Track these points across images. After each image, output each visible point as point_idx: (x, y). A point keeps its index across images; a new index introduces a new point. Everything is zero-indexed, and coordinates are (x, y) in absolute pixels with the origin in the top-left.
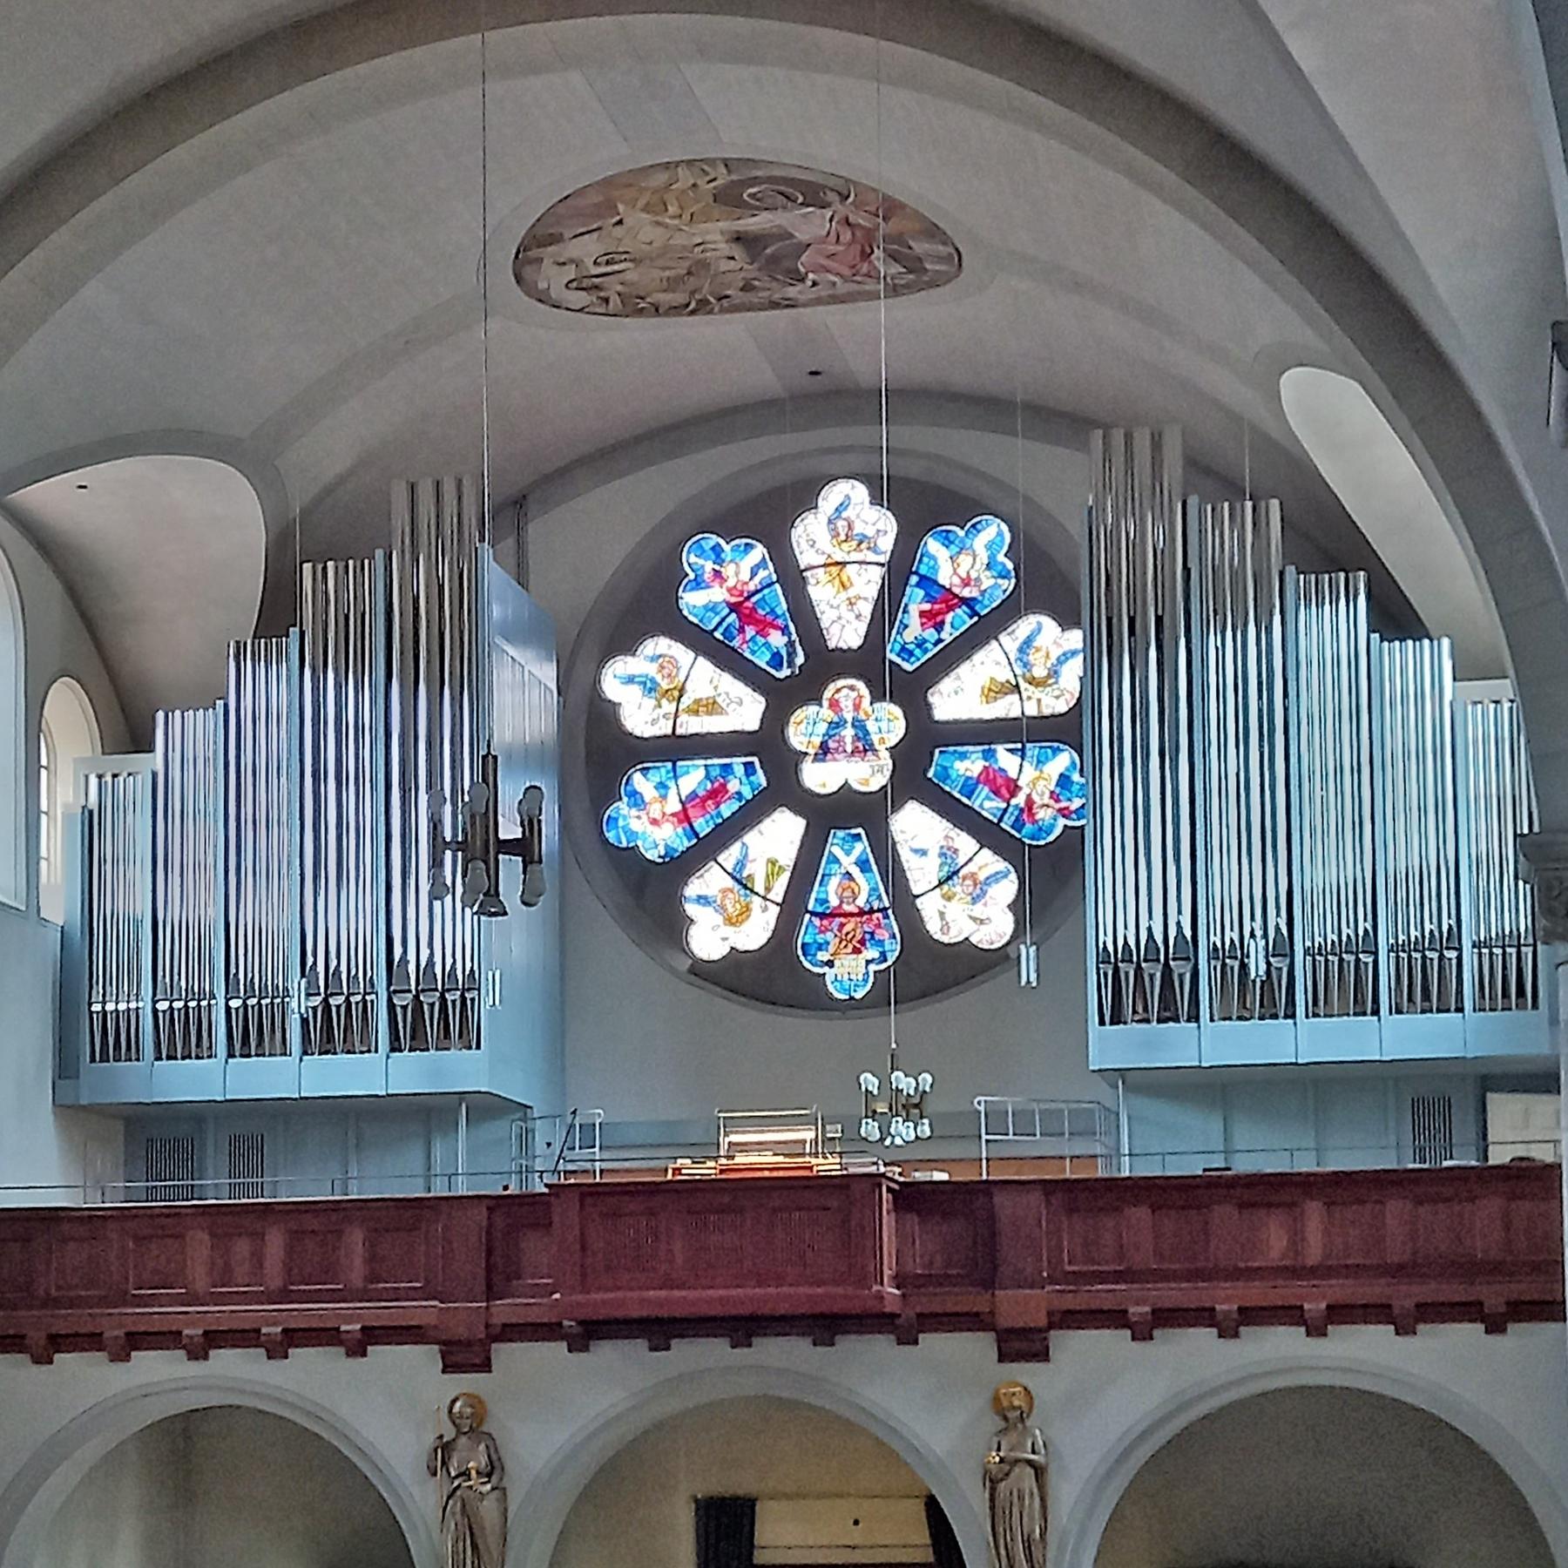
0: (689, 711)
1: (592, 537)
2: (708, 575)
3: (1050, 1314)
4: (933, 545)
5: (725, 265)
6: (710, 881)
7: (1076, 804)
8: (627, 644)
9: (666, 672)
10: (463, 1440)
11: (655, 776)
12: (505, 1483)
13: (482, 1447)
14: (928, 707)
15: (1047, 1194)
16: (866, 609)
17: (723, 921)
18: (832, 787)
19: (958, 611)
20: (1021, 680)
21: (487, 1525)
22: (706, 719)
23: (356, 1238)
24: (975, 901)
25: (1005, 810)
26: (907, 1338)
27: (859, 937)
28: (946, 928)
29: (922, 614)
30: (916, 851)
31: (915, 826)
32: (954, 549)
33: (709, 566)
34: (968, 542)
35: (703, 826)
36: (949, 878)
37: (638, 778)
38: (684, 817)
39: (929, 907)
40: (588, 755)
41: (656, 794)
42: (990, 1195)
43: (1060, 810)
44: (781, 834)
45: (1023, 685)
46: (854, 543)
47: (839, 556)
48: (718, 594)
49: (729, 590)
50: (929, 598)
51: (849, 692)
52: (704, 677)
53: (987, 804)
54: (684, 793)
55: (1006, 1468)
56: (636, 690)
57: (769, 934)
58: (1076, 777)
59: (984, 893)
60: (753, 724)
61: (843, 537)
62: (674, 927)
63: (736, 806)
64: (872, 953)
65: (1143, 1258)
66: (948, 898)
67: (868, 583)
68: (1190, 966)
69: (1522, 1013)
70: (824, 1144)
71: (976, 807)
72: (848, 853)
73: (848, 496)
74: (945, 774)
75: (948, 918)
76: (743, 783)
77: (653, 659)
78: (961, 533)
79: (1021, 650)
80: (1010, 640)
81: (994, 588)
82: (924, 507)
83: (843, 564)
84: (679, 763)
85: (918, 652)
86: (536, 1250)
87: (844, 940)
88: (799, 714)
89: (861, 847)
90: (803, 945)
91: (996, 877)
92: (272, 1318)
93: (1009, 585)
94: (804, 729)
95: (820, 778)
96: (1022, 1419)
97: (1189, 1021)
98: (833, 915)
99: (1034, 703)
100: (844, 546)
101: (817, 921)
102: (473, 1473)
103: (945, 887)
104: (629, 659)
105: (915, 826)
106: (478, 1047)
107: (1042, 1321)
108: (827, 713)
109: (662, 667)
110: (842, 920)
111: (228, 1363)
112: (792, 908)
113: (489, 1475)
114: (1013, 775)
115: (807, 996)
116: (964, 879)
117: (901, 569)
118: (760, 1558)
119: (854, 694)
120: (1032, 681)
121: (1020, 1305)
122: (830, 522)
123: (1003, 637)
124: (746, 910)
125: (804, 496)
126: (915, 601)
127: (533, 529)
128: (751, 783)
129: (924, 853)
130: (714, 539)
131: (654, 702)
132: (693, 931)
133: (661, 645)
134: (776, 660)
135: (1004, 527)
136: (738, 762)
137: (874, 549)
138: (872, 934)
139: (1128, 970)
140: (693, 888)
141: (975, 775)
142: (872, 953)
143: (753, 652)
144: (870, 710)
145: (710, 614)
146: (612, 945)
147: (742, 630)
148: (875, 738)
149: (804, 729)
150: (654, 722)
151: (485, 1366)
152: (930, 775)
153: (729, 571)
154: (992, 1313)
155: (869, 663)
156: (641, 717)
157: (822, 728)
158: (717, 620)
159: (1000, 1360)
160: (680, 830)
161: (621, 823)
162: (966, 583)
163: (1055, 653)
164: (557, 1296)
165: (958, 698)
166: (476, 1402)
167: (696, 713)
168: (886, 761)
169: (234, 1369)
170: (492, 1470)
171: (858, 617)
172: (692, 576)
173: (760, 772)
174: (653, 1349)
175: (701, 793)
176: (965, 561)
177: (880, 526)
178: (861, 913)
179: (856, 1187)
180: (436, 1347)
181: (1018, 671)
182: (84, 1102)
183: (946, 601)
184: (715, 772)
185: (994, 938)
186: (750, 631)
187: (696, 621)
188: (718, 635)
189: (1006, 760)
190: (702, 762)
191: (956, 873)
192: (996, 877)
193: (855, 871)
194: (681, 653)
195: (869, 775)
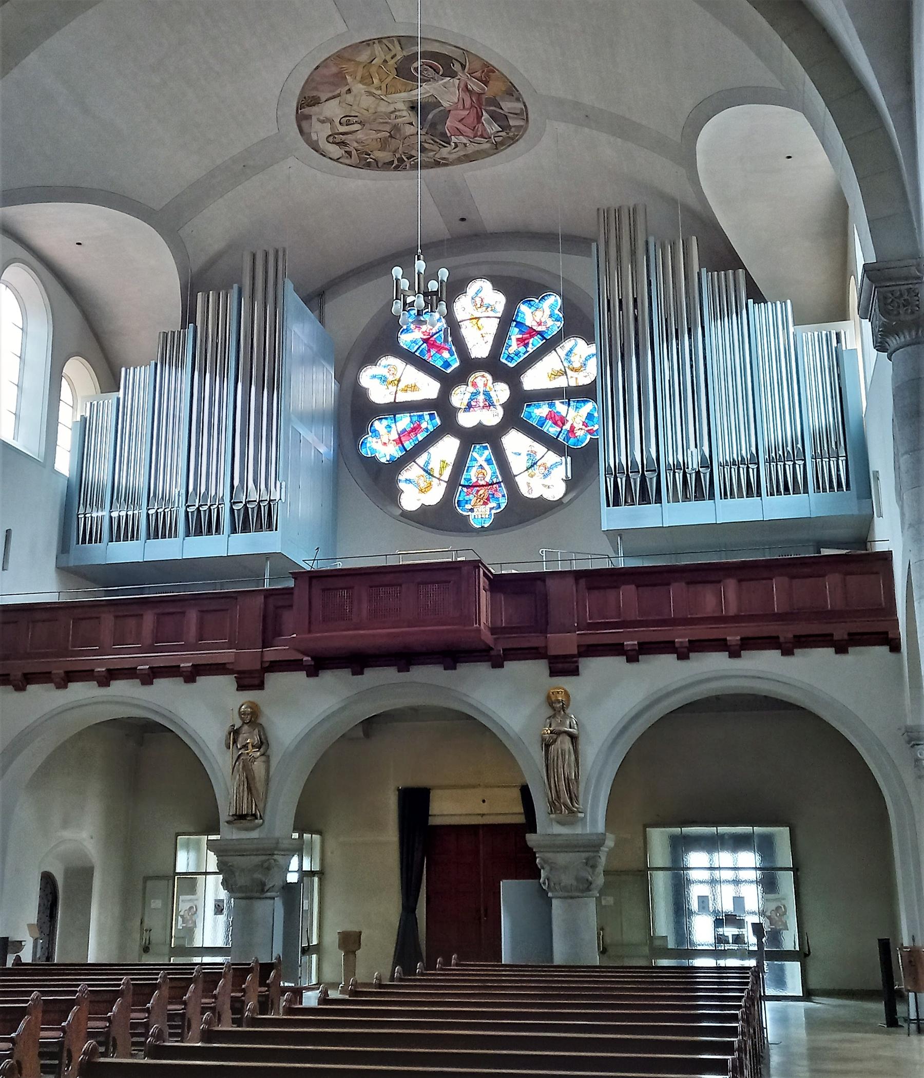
1: (354, 309)
4: (523, 308)
5: (409, 130)
6: (412, 472)
7: (596, 427)
10: (246, 727)
11: (385, 422)
12: (269, 752)
13: (256, 731)
14: (520, 383)
16: (490, 339)
17: (418, 491)
21: (257, 779)
23: (193, 616)
24: (545, 476)
26: (497, 664)
29: (518, 340)
35: (409, 445)
36: (532, 466)
37: (377, 425)
38: (399, 441)
40: (352, 412)
41: (386, 430)
42: (544, 581)
43: (588, 431)
44: (448, 447)
47: (477, 315)
50: (521, 332)
51: (482, 379)
52: (411, 374)
53: (551, 429)
54: (400, 430)
55: (555, 736)
56: (377, 381)
58: (596, 415)
59: (549, 473)
62: (392, 494)
63: (426, 434)
65: (633, 615)
67: (491, 327)
72: (481, 456)
76: (429, 423)
79: (567, 355)
80: (562, 350)
81: (554, 327)
82: (519, 290)
83: (479, 318)
85: (516, 358)
86: (289, 619)
87: (479, 498)
89: (488, 453)
91: (556, 465)
92: (145, 661)
93: (560, 324)
94: (459, 397)
95: (467, 420)
101: (465, 489)
102: (250, 746)
103: (530, 471)
112: (454, 483)
113: (260, 748)
117: (507, 320)
121: (563, 642)
124: (430, 486)
126: (515, 333)
127: (329, 307)
136: (426, 415)
139: (622, 482)
140: (404, 475)
142: (493, 504)
146: (358, 498)
147: (429, 351)
148: (494, 399)
149: (459, 397)
154: (546, 647)
155: (493, 365)
156: (379, 395)
157: (468, 396)
161: (368, 445)
162: (539, 324)
165: (533, 380)
168: (500, 412)
170: (263, 744)
174: (354, 674)
176: (539, 314)
178: (488, 485)
179: (465, 570)
181: (566, 364)
183: (530, 333)
184: (415, 419)
189: (560, 407)
191: (535, 463)
192: (556, 465)
193: (485, 465)
195: (492, 418)
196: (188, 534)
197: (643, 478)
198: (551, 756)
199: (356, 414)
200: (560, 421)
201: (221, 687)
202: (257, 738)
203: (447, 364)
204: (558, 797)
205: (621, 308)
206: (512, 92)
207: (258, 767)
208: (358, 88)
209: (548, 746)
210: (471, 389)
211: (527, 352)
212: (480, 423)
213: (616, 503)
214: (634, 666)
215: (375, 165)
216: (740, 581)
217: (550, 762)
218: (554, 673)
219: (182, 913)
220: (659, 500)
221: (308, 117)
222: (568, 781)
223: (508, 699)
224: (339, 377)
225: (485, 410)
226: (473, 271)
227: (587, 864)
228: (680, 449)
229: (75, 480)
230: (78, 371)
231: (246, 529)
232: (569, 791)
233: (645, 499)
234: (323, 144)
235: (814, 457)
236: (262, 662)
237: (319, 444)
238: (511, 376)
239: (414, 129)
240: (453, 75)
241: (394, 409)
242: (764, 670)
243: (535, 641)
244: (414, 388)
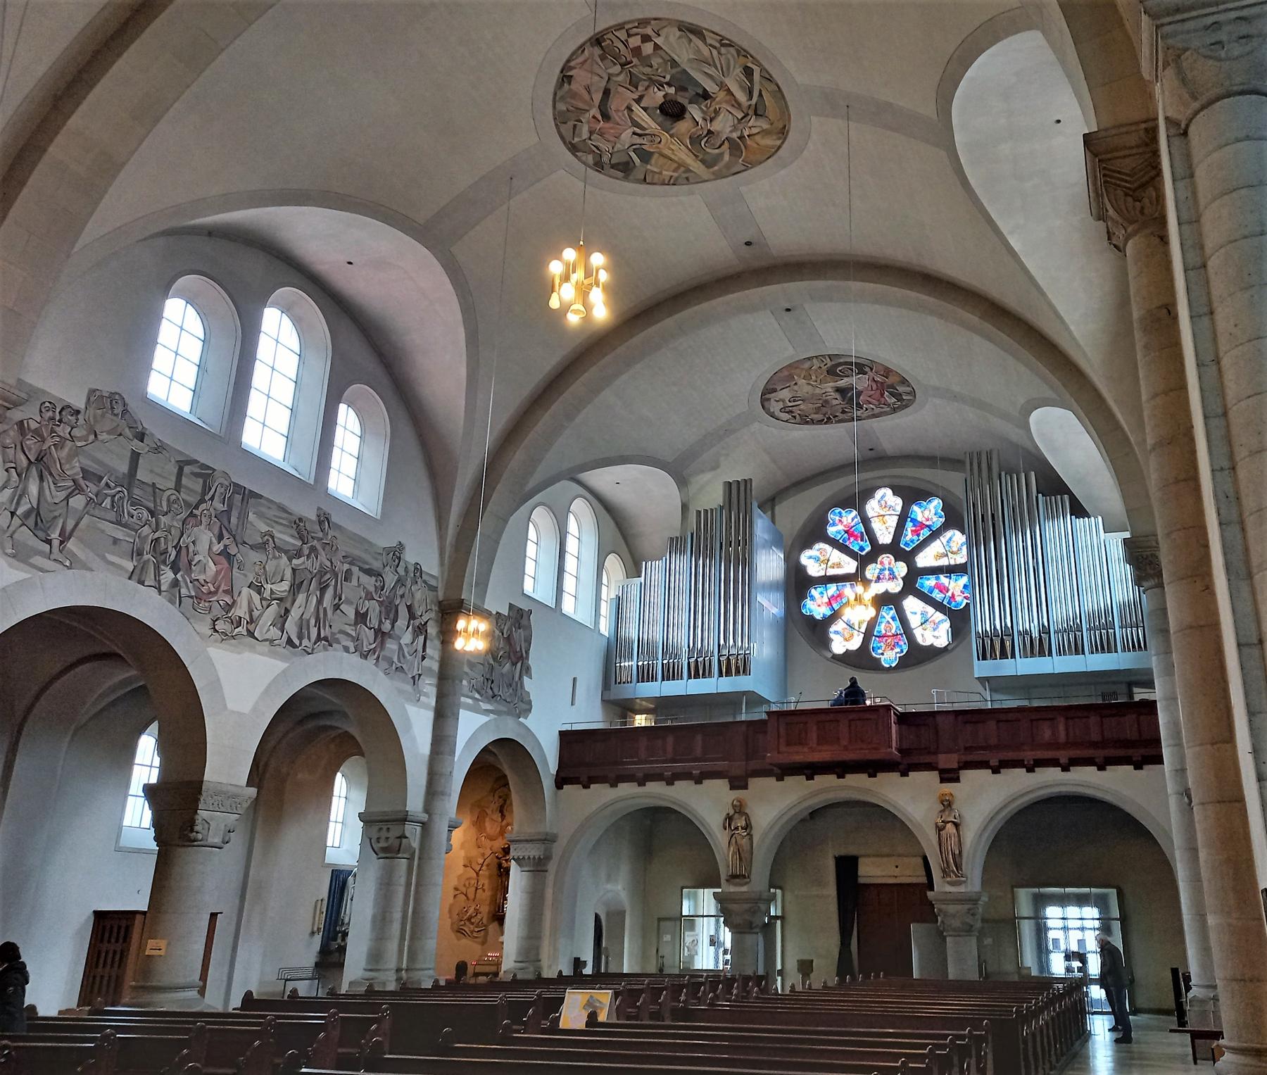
1: (795, 512)
6: (838, 626)
8: (807, 543)
16: (892, 530)
17: (842, 642)
26: (904, 774)
28: (924, 640)
37: (813, 592)
38: (829, 603)
48: (840, 527)
51: (887, 559)
52: (836, 556)
53: (937, 595)
60: (853, 570)
62: (825, 642)
64: (898, 650)
67: (893, 522)
73: (885, 494)
81: (938, 522)
82: (911, 495)
89: (893, 612)
91: (942, 621)
98: (884, 636)
105: (912, 605)
108: (879, 566)
112: (868, 635)
124: (852, 635)
125: (868, 493)
126: (909, 525)
127: (777, 508)
133: (822, 545)
134: (862, 549)
140: (833, 628)
142: (898, 650)
146: (803, 647)
151: (745, 787)
153: (844, 519)
155: (895, 549)
156: (814, 570)
159: (941, 782)
169: (656, 792)
170: (748, 827)
176: (926, 513)
182: (612, 698)
189: (943, 579)
192: (942, 621)
196: (690, 677)
197: (1002, 640)
199: (798, 583)
200: (943, 589)
201: (721, 785)
202: (744, 823)
203: (862, 549)
206: (904, 381)
208: (802, 382)
210: (879, 566)
213: (984, 658)
215: (813, 422)
220: (1013, 656)
221: (769, 399)
222: (953, 854)
224: (786, 559)
226: (878, 483)
228: (1027, 622)
229: (613, 639)
230: (613, 562)
233: (1004, 655)
234: (777, 413)
237: (771, 606)
238: (906, 556)
239: (836, 400)
240: (865, 373)
244: (839, 565)
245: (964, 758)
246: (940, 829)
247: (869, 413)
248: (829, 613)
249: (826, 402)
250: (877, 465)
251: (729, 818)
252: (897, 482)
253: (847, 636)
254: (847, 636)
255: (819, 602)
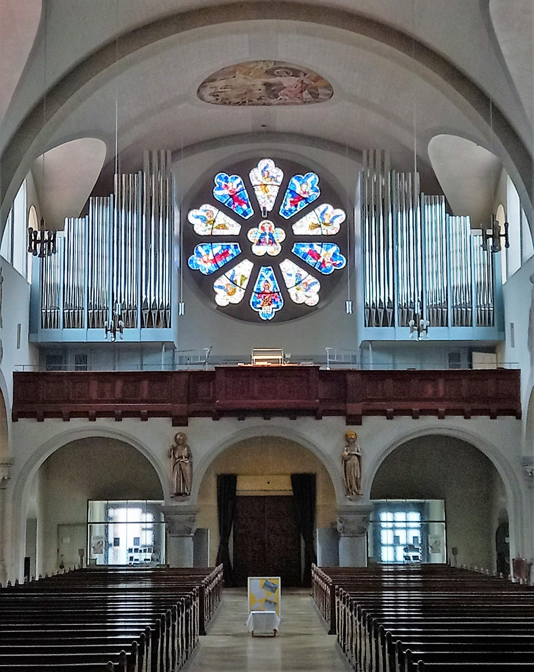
0: (216, 228)
1: (186, 173)
2: (223, 186)
3: (363, 410)
4: (294, 180)
6: (222, 281)
7: (338, 262)
9: (209, 215)
10: (179, 447)
13: (186, 449)
15: (362, 374)
16: (273, 199)
18: (262, 253)
19: (302, 201)
20: (321, 224)
22: (222, 230)
24: (307, 290)
25: (316, 263)
26: (319, 418)
27: (270, 300)
28: (297, 298)
29: (291, 202)
30: (288, 275)
31: (288, 267)
32: (301, 182)
33: (224, 183)
34: (305, 181)
35: (221, 264)
36: (299, 282)
37: (200, 248)
38: (214, 261)
39: (292, 292)
41: (205, 253)
42: (345, 375)
43: (333, 264)
44: (245, 268)
45: (322, 225)
46: (269, 179)
47: (265, 182)
48: (226, 192)
49: (230, 191)
50: (293, 197)
51: (267, 224)
52: (221, 218)
53: (310, 261)
56: (199, 220)
57: (242, 299)
58: (338, 254)
59: (309, 288)
60: (237, 232)
61: (266, 177)
63: (231, 258)
64: (275, 306)
66: (298, 289)
67: (274, 191)
68: (392, 310)
69: (489, 328)
70: (285, 359)
71: (307, 262)
74: (297, 251)
75: (298, 295)
77: (205, 211)
78: (303, 178)
79: (321, 214)
82: (292, 169)
83: (266, 185)
84: (213, 244)
85: (289, 213)
87: (266, 301)
88: (252, 230)
89: (272, 272)
90: (253, 302)
91: (313, 284)
93: (318, 194)
94: (253, 235)
95: (258, 250)
96: (354, 442)
97: (391, 326)
99: (325, 231)
100: (267, 179)
101: (257, 295)
102: (184, 457)
103: (298, 286)
104: (197, 210)
105: (288, 267)
106: (170, 327)
107: (360, 412)
108: (262, 232)
109: (207, 214)
110: (265, 295)
111: (101, 422)
114: (319, 252)
115: (255, 318)
116: (304, 283)
117: (284, 188)
118: (238, 494)
119: (269, 225)
120: (325, 224)
121: (354, 408)
122: (262, 172)
123: (316, 210)
124: (234, 291)
126: (289, 198)
128: (236, 251)
129: (291, 275)
130: (225, 175)
131: (205, 225)
132: (217, 296)
133: (207, 207)
135: (317, 177)
136: (232, 245)
137: (276, 181)
138: (274, 300)
140: (217, 283)
141: (307, 252)
143: (237, 211)
144: (274, 230)
145: (224, 198)
147: (234, 204)
148: (276, 239)
149: (253, 235)
150: (205, 231)
152: (293, 251)
153: (230, 185)
155: (274, 216)
156: (201, 229)
157: (259, 235)
158: (225, 200)
160: (213, 265)
161: (194, 262)
162: (305, 193)
163: (332, 216)
164: (218, 401)
165: (301, 228)
166: (182, 435)
167: (219, 229)
170: (189, 456)
171: (271, 201)
172: (218, 186)
173: (239, 248)
175: (220, 253)
176: (304, 186)
177: (278, 174)
178: (271, 293)
180: (171, 418)
181: (321, 221)
184: (225, 247)
185: (312, 302)
186: (236, 204)
187: (219, 200)
188: (226, 205)
189: (316, 247)
190: (221, 244)
191: (300, 282)
192: (313, 284)
193: (269, 280)
194: (215, 211)
195: (274, 250)
197: (385, 311)
198: (347, 466)
201: (164, 423)
203: (245, 213)
204: (351, 486)
205: (375, 210)
207: (188, 468)
209: (346, 461)
211: (296, 210)
212: (266, 253)
214: (389, 421)
216: (446, 380)
217: (347, 469)
218: (348, 423)
219: (93, 545)
220: (393, 325)
223: (323, 437)
225: (270, 245)
227: (363, 520)
231: (150, 325)
232: (357, 484)
233: (385, 324)
235: (477, 307)
236: (188, 411)
238: (286, 225)
241: (211, 239)
242: (456, 425)
243: (341, 407)
244: (224, 227)
245: (367, 407)
246: (345, 461)
247: (281, 101)
248: (214, 269)
249: (251, 91)
250: (265, 139)
251: (174, 449)
252: (279, 155)
253: (230, 291)
254: (230, 291)
255: (205, 258)
